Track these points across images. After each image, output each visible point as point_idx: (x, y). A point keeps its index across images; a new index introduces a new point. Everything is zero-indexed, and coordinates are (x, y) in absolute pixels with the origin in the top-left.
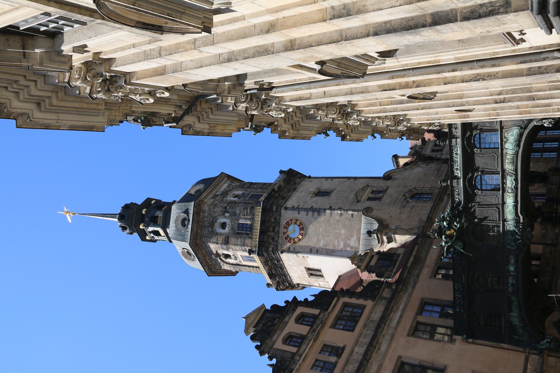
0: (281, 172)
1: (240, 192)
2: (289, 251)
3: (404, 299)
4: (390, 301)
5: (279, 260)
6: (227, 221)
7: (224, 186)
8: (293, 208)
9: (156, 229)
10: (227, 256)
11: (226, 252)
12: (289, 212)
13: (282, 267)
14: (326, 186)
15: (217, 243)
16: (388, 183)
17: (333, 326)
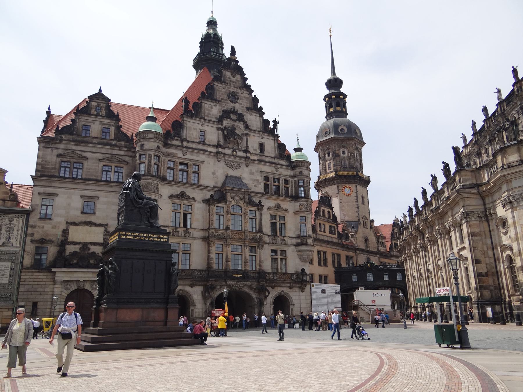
0: (369, 177)
1: (358, 157)
2: (338, 189)
3: (339, 248)
4: (338, 243)
5: (333, 184)
6: (346, 155)
7: (360, 147)
8: (356, 189)
9: (333, 106)
10: (329, 154)
11: (331, 154)
12: (355, 187)
13: (329, 185)
14: (365, 200)
15: (335, 151)
16: (369, 227)
17: (330, 226)
